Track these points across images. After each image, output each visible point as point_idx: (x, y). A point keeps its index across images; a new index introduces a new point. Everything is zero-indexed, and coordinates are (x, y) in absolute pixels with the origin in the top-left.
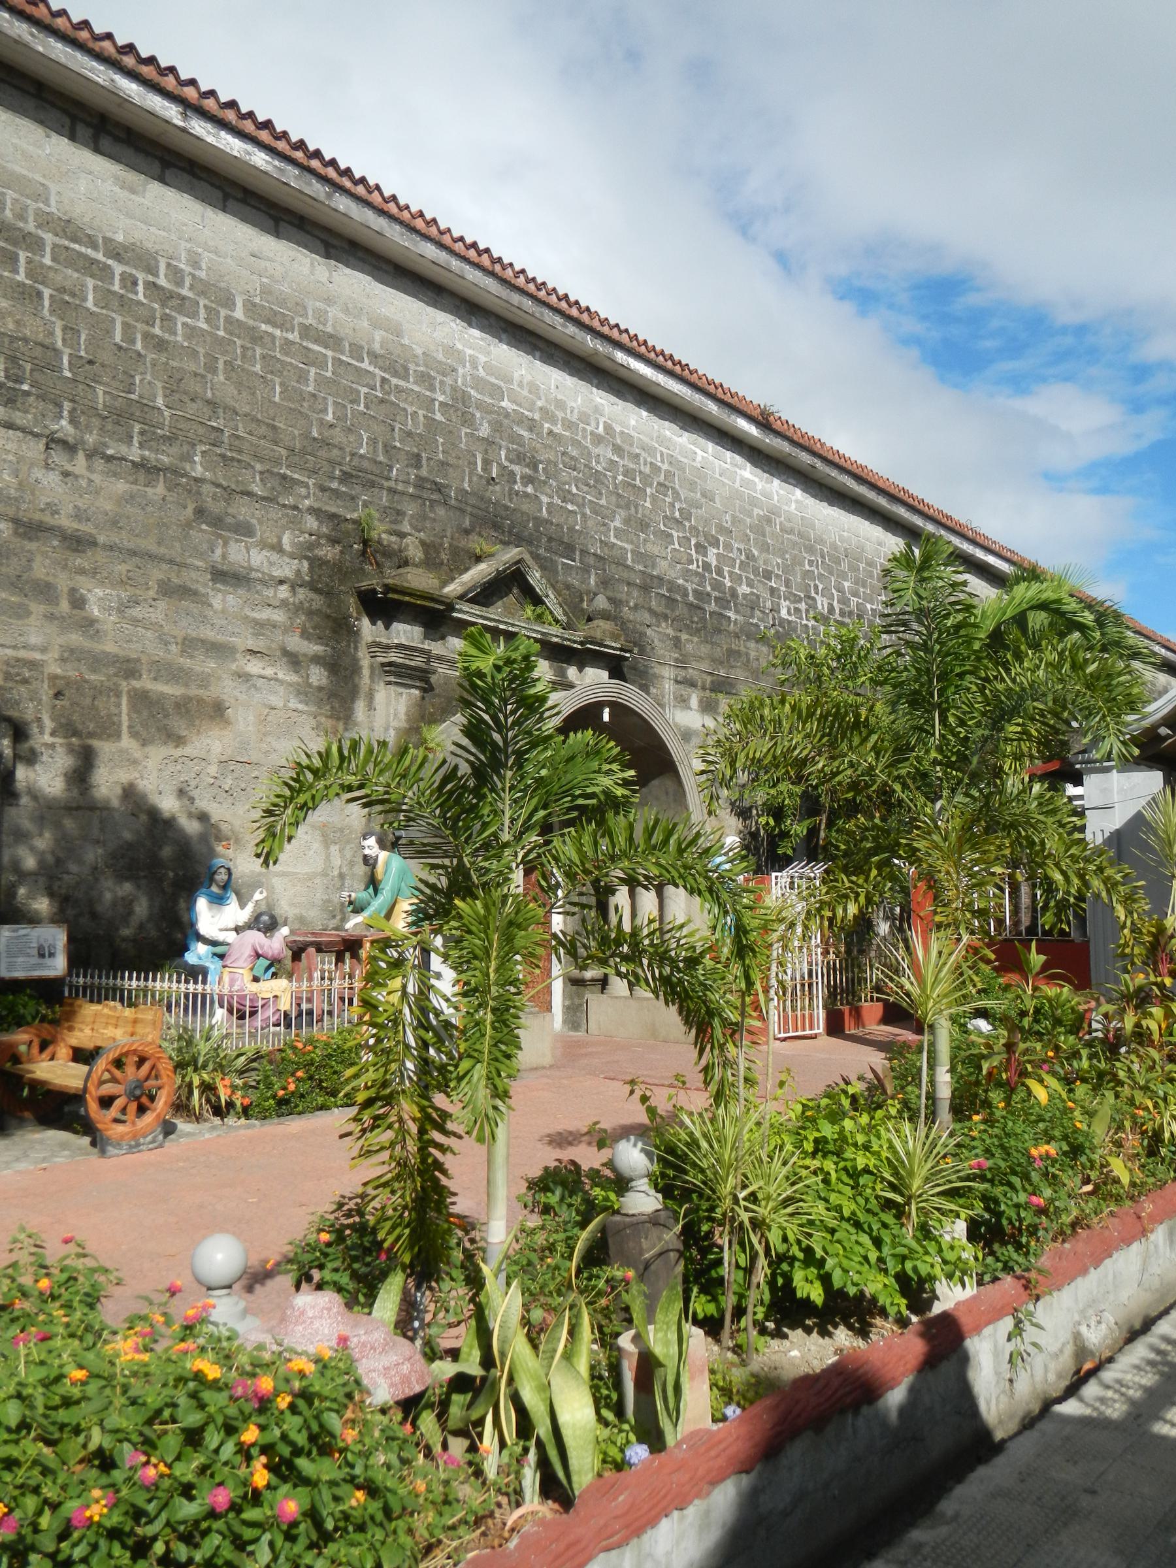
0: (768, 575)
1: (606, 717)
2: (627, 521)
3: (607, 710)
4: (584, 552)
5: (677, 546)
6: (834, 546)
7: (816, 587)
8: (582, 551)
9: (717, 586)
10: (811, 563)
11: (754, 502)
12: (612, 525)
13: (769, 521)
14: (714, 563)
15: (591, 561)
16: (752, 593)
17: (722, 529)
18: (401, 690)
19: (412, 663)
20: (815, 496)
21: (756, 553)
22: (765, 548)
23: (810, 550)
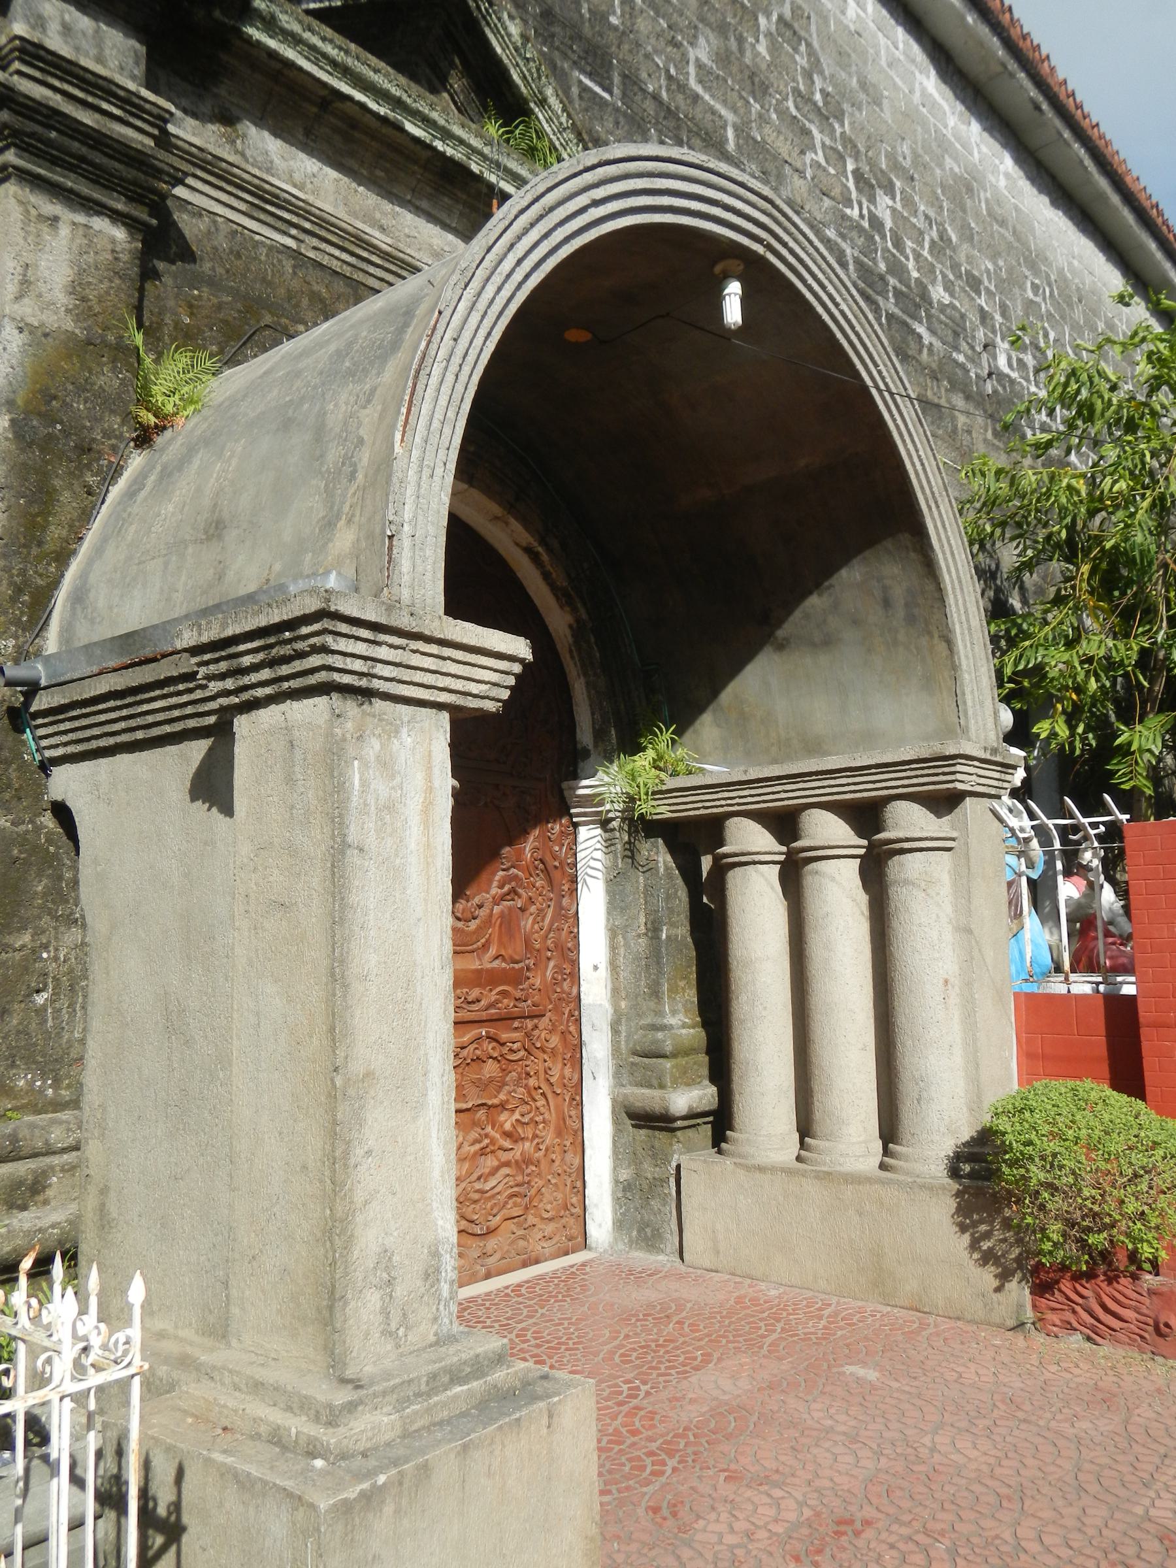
0: (974, 284)
1: (733, 312)
2: (723, 58)
3: (734, 288)
4: (631, 82)
5: (821, 158)
6: (1061, 272)
7: (1046, 335)
8: (624, 76)
9: (897, 269)
10: (1035, 288)
11: (944, 145)
12: (692, 54)
13: (970, 190)
14: (888, 224)
15: (649, 106)
16: (952, 306)
17: (896, 166)
18: (51, 207)
19: (87, 118)
20: (1032, 180)
21: (954, 239)
22: (967, 235)
23: (1033, 266)
